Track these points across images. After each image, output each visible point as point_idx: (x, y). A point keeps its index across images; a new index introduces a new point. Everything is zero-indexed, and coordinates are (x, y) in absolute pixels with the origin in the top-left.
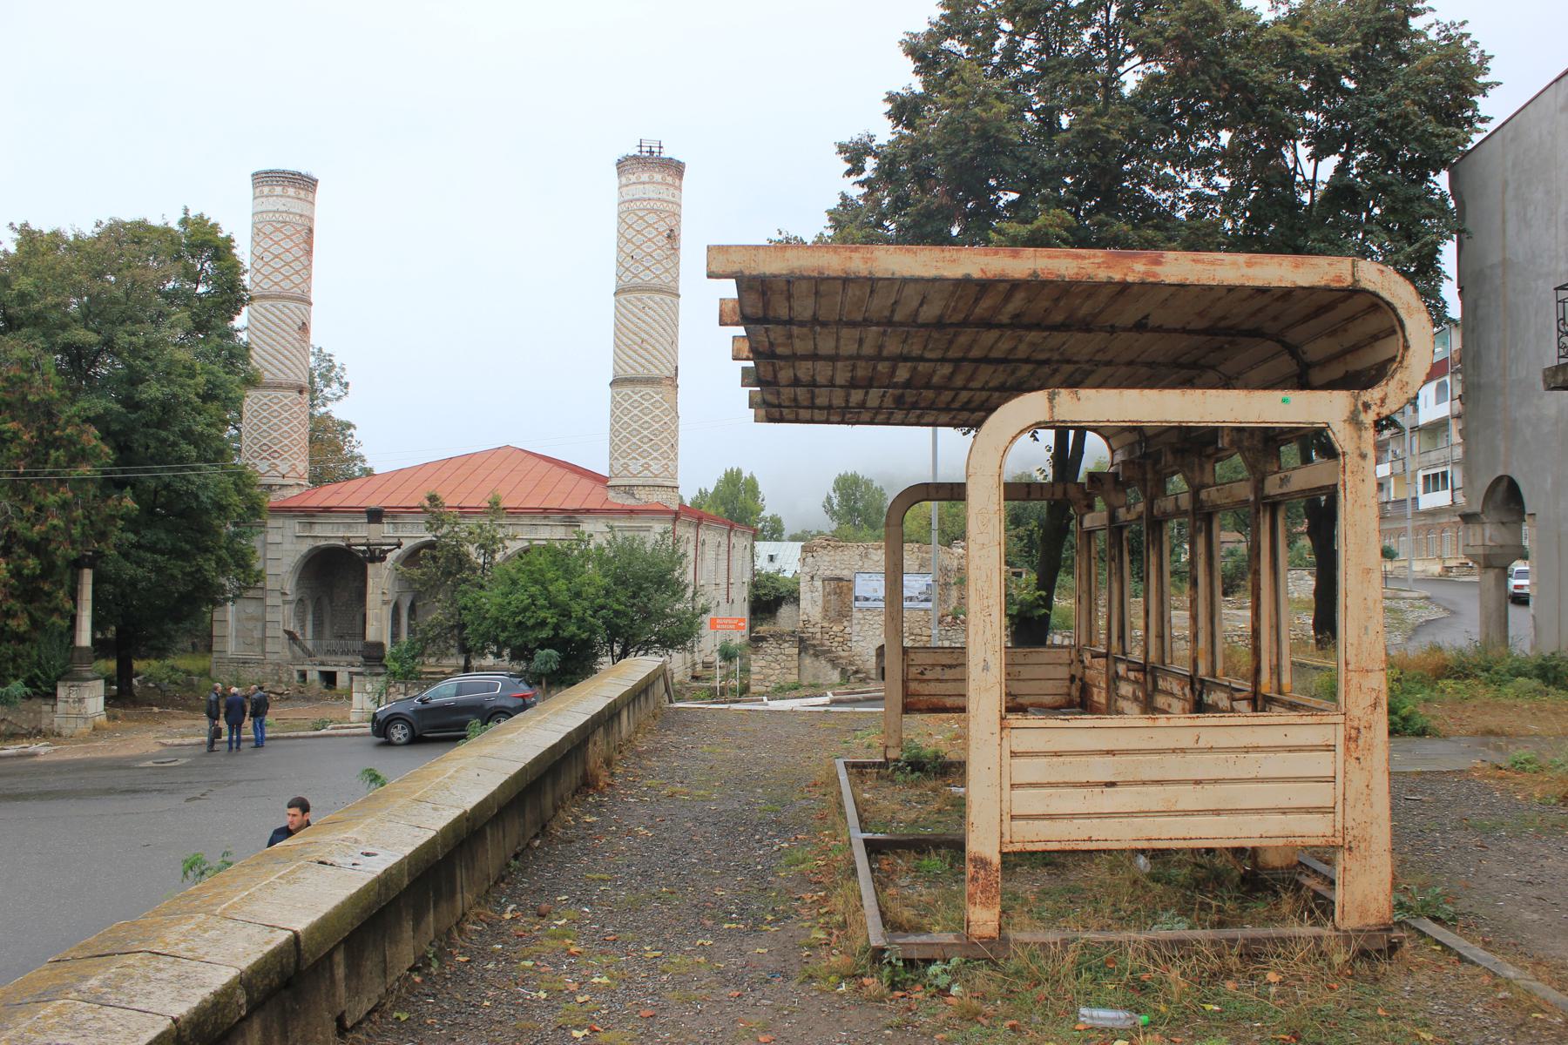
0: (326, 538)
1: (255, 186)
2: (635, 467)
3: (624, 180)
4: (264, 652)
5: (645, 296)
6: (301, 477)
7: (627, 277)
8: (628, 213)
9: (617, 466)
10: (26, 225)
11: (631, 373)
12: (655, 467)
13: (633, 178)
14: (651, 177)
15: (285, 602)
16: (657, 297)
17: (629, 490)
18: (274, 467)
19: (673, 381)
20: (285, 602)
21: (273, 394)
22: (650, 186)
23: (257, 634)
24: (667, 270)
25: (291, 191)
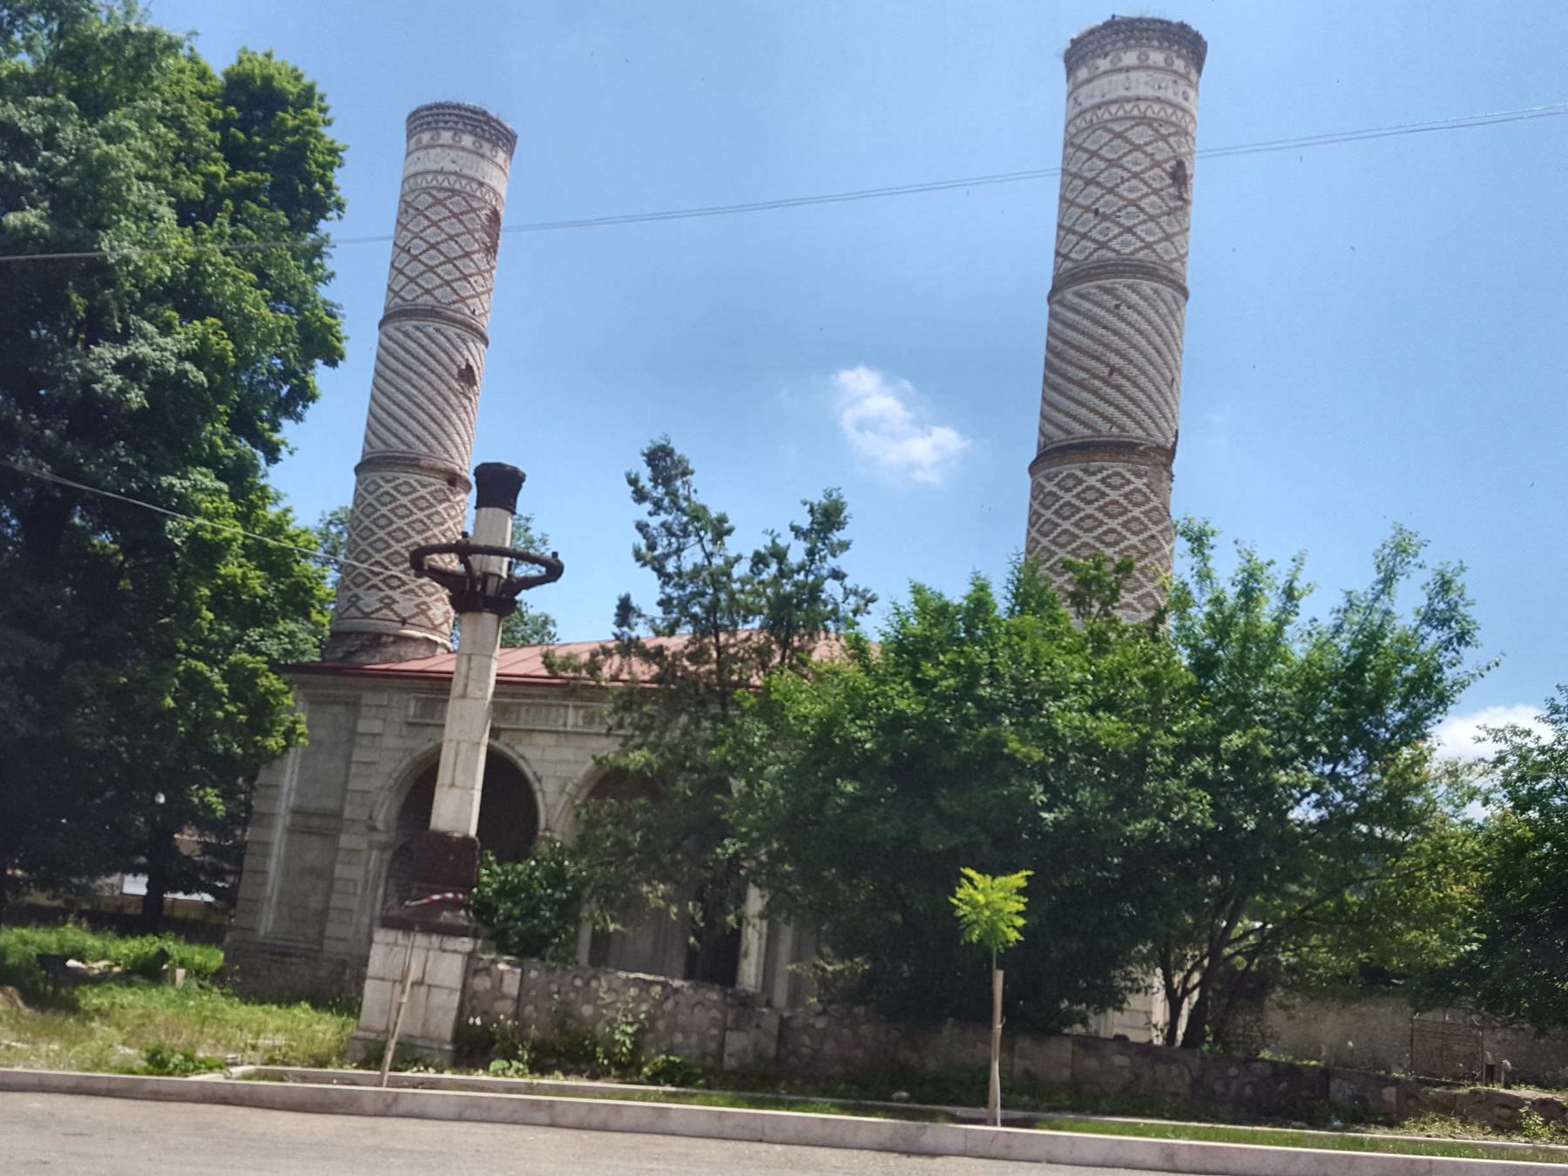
3: (1083, 74)
5: (1120, 284)
6: (435, 629)
13: (1104, 64)
14: (1143, 58)
16: (1146, 286)
18: (389, 603)
21: (403, 477)
24: (1168, 238)
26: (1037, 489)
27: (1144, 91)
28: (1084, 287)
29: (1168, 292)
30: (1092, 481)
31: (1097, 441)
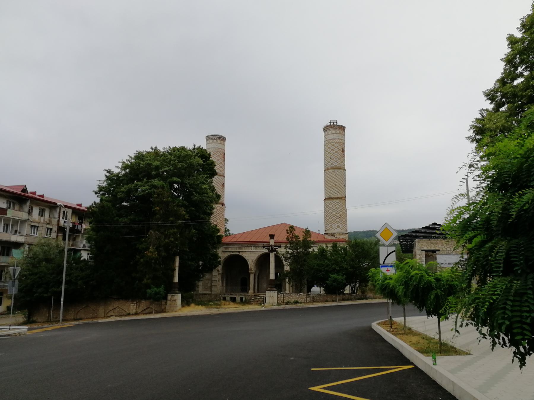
0: (233, 252)
1: (207, 140)
2: (334, 227)
3: (326, 133)
4: (211, 291)
5: (335, 170)
7: (329, 165)
8: (328, 145)
9: (328, 227)
10: (156, 147)
11: (332, 196)
12: (341, 227)
13: (330, 132)
15: (219, 274)
16: (339, 171)
17: (333, 234)
19: (343, 198)
20: (219, 274)
22: (334, 135)
23: (209, 285)
25: (219, 141)
26: (325, 205)
27: (337, 138)
28: (330, 171)
29: (343, 171)
30: (334, 204)
31: (335, 197)
